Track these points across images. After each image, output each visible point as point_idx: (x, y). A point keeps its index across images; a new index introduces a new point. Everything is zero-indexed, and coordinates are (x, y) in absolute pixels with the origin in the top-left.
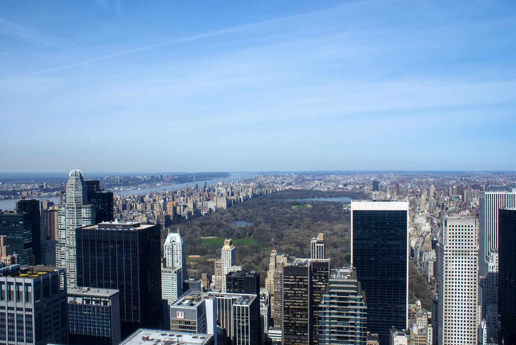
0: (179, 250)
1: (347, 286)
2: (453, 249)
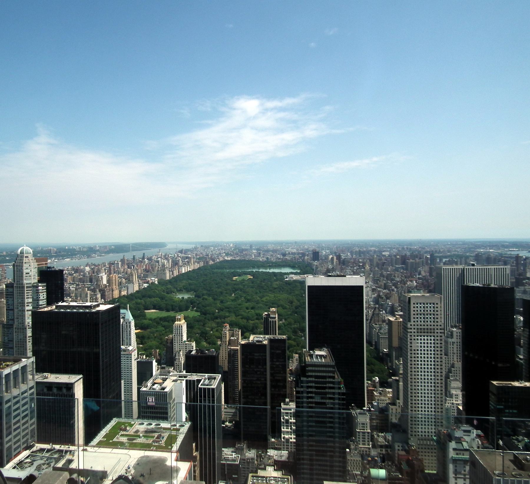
1: (324, 369)
2: (418, 327)
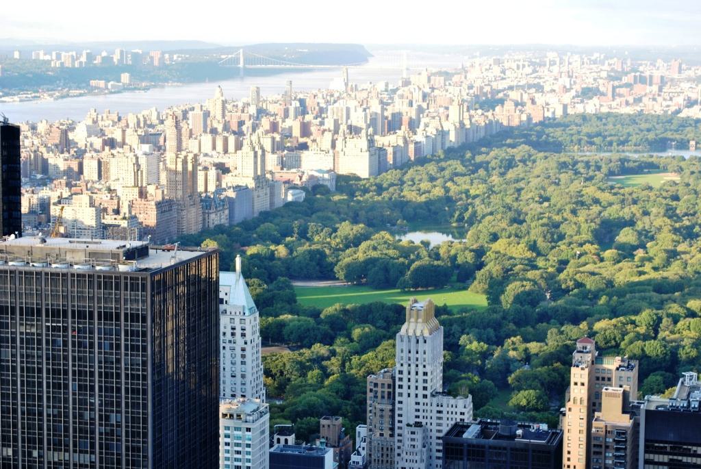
0: (238, 332)
